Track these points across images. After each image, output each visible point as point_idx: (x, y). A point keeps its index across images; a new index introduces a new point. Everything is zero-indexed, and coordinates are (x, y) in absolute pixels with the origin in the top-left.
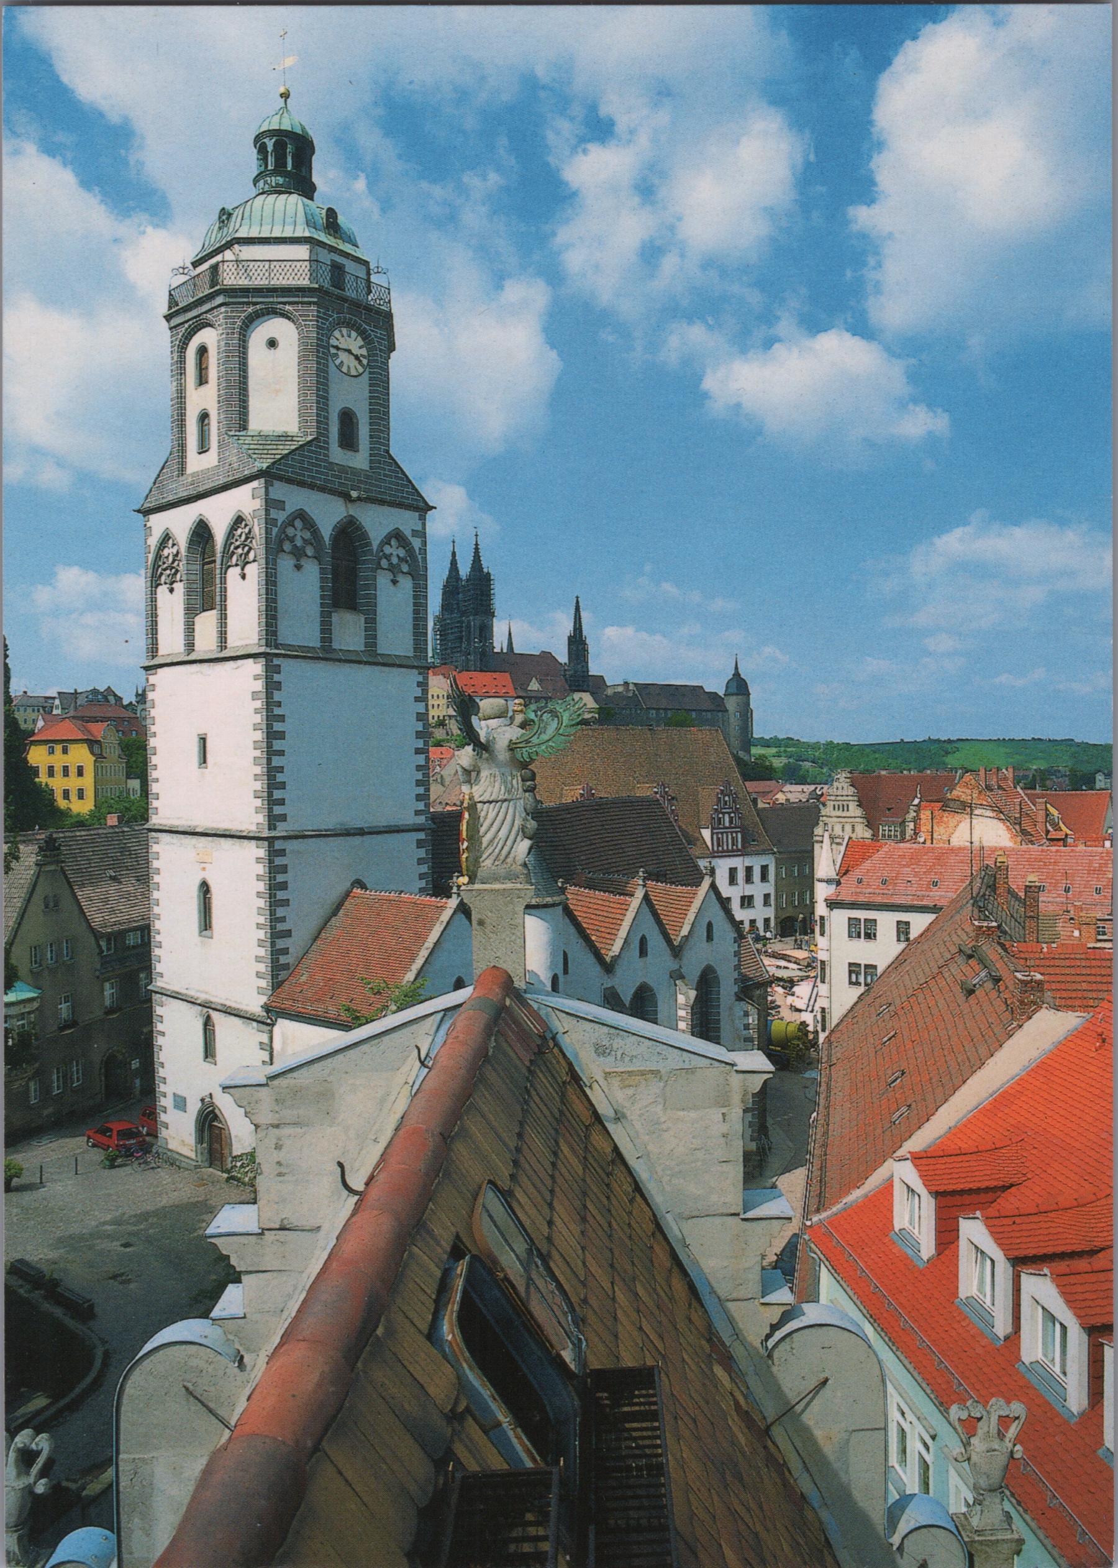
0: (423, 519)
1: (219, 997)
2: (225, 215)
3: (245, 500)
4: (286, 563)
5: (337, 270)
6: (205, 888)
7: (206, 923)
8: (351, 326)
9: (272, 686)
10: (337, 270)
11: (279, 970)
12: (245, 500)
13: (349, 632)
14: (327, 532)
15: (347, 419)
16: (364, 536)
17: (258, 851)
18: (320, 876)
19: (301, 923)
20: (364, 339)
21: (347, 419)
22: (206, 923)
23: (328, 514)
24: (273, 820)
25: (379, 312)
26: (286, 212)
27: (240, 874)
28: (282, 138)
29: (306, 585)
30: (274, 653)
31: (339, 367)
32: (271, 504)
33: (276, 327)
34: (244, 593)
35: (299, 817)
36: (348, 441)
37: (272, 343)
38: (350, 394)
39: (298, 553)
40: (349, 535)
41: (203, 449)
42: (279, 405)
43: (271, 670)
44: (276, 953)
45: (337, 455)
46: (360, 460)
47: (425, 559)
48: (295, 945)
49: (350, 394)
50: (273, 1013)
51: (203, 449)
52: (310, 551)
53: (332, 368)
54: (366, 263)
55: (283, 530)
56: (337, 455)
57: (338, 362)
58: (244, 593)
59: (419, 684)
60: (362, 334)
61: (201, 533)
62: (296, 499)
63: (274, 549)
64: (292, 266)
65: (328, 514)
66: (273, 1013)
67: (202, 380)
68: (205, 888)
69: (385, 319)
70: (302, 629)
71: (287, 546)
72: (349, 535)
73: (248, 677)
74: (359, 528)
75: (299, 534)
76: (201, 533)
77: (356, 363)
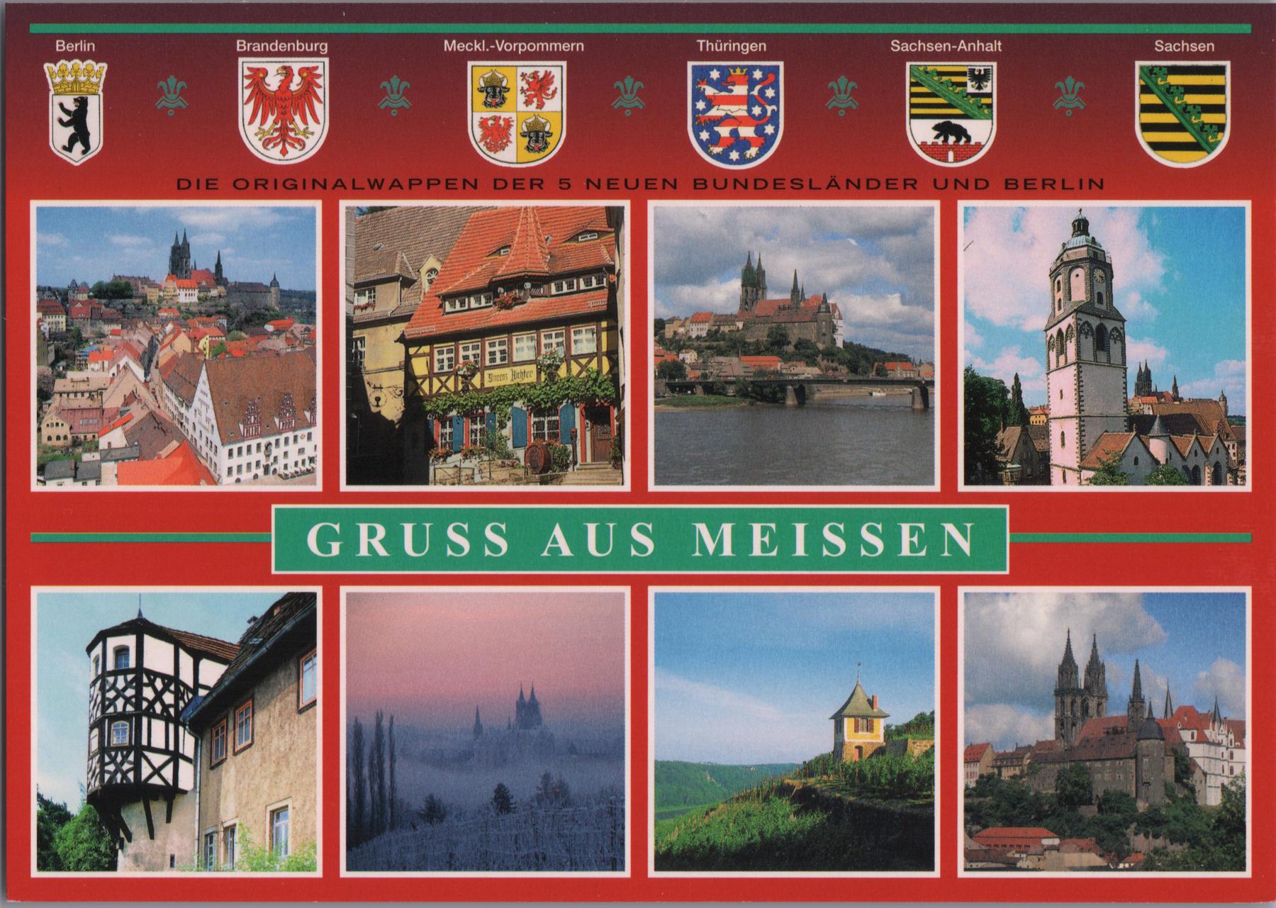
1: (1069, 465)
2: (1064, 245)
3: (1070, 320)
4: (1083, 336)
5: (1095, 254)
6: (1063, 434)
7: (1063, 444)
9: (1079, 372)
10: (1095, 254)
11: (1082, 457)
12: (1070, 320)
13: (1102, 356)
15: (1100, 295)
17: (1075, 421)
18: (1093, 432)
19: (1089, 440)
21: (1100, 295)
22: (1063, 444)
23: (1095, 322)
24: (1080, 411)
26: (1081, 240)
27: (1071, 428)
28: (1079, 221)
29: (1088, 343)
30: (1079, 363)
32: (1077, 319)
33: (1080, 271)
34: (1071, 347)
35: (1088, 410)
36: (1100, 301)
38: (1101, 288)
39: (1087, 334)
40: (1101, 328)
41: (1060, 308)
42: (1080, 293)
43: (1079, 367)
44: (1082, 451)
45: (1097, 305)
46: (1103, 307)
48: (1088, 448)
49: (1101, 288)
50: (1081, 468)
51: (1060, 308)
56: (1097, 305)
58: (1071, 347)
61: (1060, 331)
62: (1085, 318)
63: (1080, 332)
64: (1083, 253)
65: (1095, 322)
66: (1081, 468)
68: (1063, 434)
69: (1110, 266)
70: (1088, 355)
72: (1101, 328)
73: (1072, 370)
75: (1086, 327)
76: (1060, 331)
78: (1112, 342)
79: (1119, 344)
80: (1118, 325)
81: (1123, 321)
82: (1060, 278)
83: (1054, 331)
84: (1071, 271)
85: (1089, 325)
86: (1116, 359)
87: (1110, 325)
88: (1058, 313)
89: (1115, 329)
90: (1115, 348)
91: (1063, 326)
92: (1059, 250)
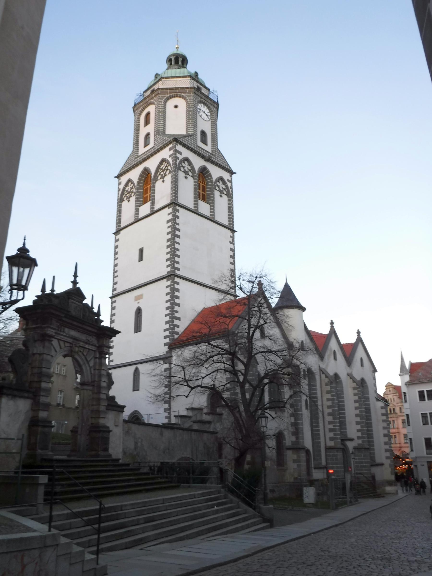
0: (231, 176)
8: (205, 104)
13: (204, 208)
14: (197, 168)
15: (203, 133)
16: (210, 175)
20: (209, 110)
25: (214, 102)
31: (201, 116)
36: (204, 141)
37: (176, 107)
46: (208, 148)
47: (232, 191)
52: (190, 174)
53: (198, 117)
54: (209, 90)
55: (180, 163)
57: (200, 114)
59: (231, 237)
60: (209, 108)
67: (147, 122)
71: (182, 169)
74: (208, 171)
77: (206, 117)
78: (217, 194)
79: (225, 198)
80: (226, 176)
81: (232, 173)
82: (151, 109)
83: (135, 175)
84: (168, 99)
85: (190, 163)
86: (222, 215)
87: (215, 172)
88: (142, 150)
89: (221, 179)
90: (221, 202)
91: (152, 164)
92: (151, 79)
